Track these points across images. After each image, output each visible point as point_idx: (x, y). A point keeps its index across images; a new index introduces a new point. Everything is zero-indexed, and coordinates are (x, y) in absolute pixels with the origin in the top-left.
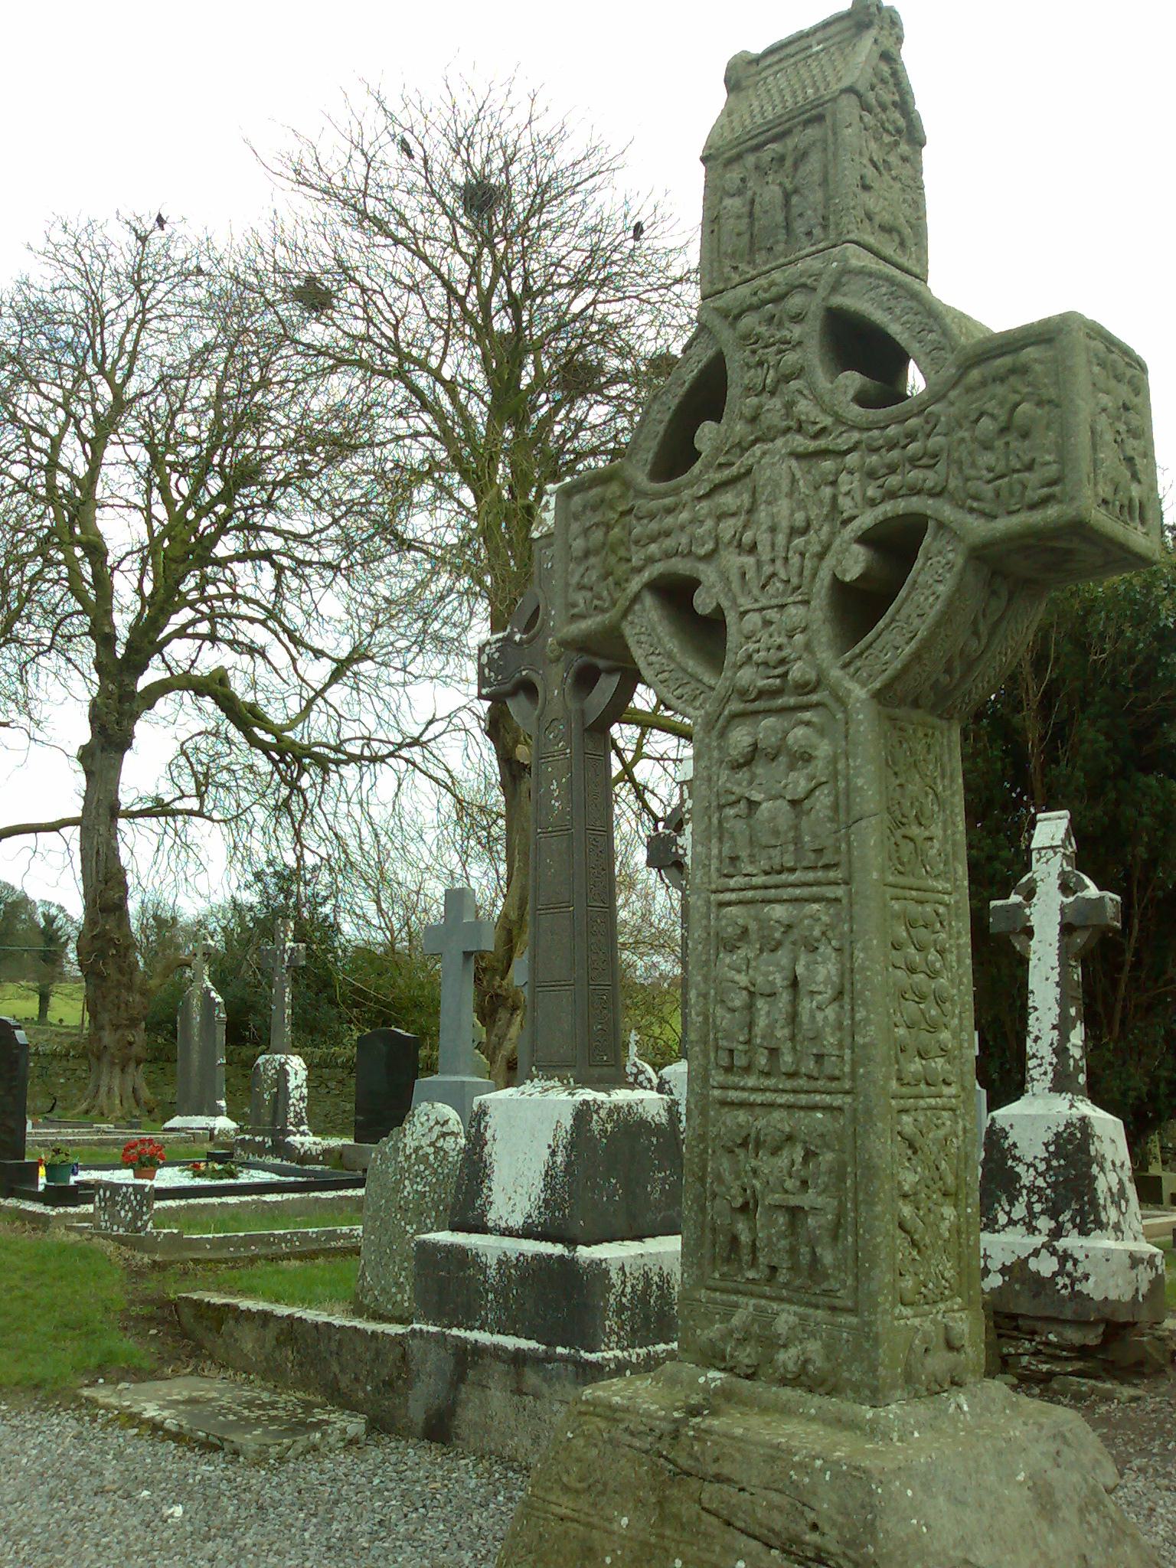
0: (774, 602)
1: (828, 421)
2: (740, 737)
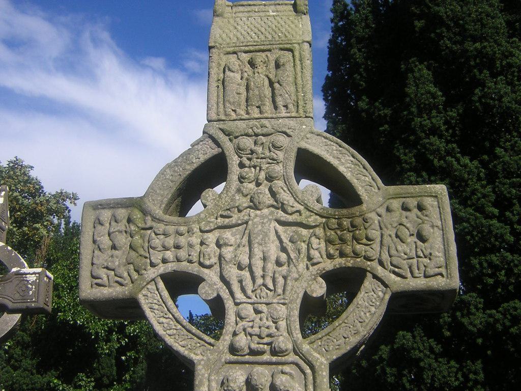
0: (263, 300)
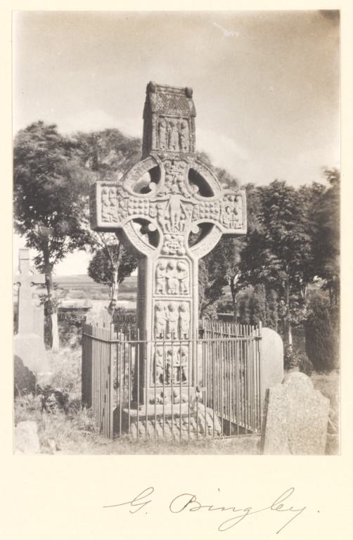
1: (190, 195)
2: (164, 263)
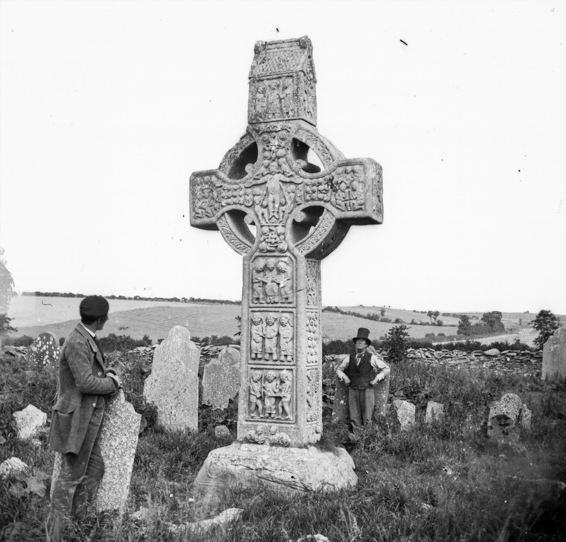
1: (292, 173)
